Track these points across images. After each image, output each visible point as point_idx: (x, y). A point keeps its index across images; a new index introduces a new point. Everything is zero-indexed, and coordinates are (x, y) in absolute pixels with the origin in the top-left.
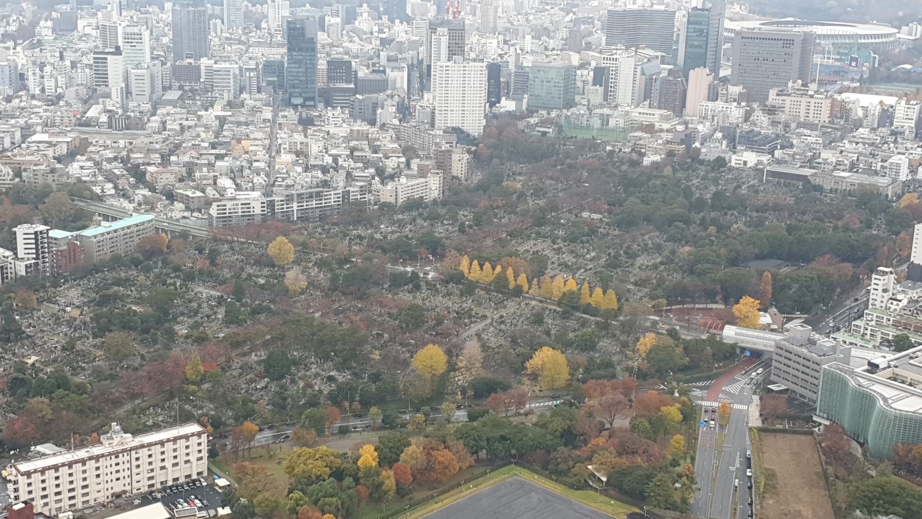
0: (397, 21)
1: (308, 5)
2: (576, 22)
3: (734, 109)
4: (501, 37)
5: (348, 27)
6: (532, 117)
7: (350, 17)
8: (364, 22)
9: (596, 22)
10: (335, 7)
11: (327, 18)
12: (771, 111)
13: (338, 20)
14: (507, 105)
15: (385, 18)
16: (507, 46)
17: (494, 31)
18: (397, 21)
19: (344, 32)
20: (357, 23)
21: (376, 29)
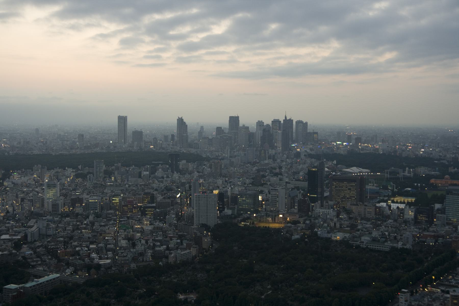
0: (175, 172)
1: (133, 166)
2: (258, 171)
3: (332, 212)
4: (224, 179)
5: (152, 176)
6: (239, 217)
7: (153, 171)
8: (159, 173)
9: (267, 171)
10: (146, 167)
11: (142, 172)
12: (348, 212)
13: (148, 173)
14: (228, 212)
15: (170, 171)
16: (226, 183)
17: (221, 175)
18: (175, 172)
19: (151, 178)
20: (156, 174)
21: (165, 176)
